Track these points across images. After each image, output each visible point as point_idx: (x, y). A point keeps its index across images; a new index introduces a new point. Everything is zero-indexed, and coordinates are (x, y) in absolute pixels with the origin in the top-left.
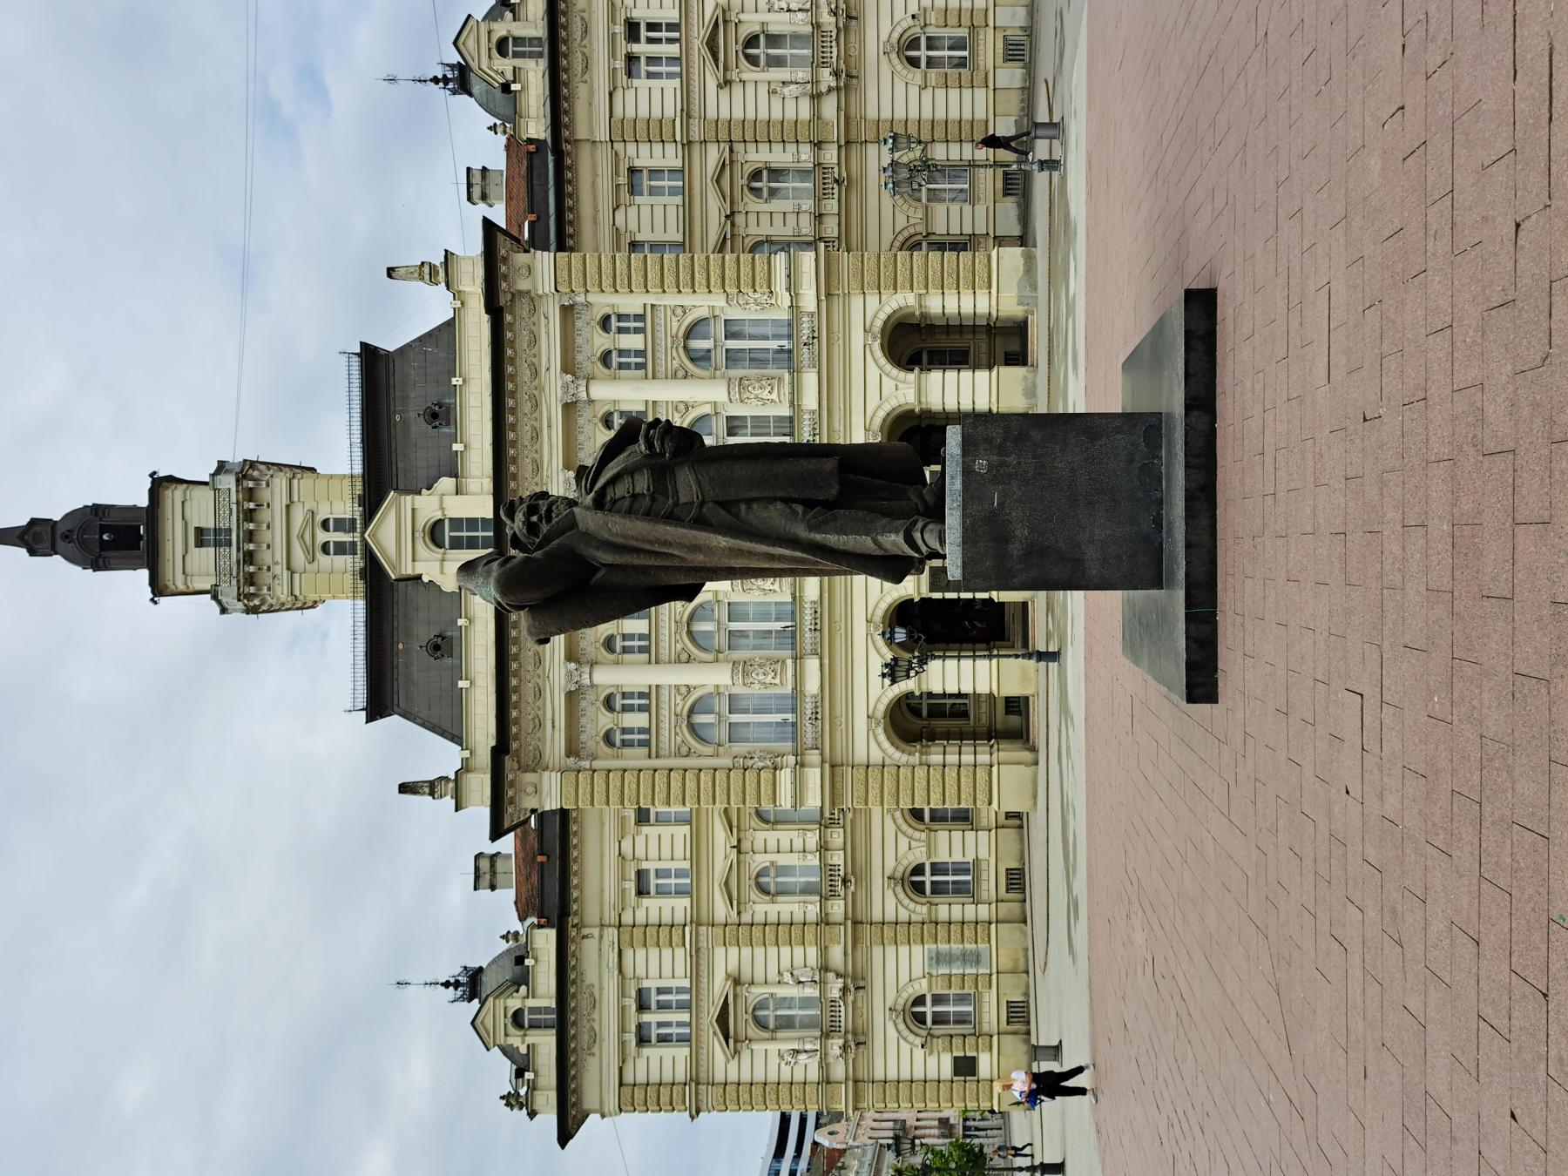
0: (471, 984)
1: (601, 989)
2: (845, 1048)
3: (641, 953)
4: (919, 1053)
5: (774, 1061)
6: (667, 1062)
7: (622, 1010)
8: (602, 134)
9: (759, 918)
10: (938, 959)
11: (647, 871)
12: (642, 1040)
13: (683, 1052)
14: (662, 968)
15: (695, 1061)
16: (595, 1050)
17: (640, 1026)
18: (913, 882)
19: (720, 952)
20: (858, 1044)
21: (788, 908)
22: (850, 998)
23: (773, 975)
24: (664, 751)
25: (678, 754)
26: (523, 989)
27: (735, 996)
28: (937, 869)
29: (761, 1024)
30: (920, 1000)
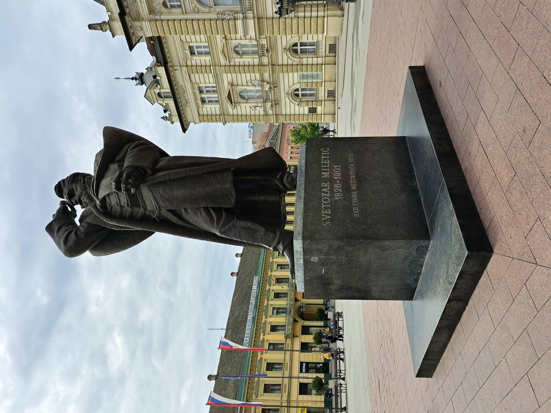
0: (140, 78)
1: (185, 87)
2: (272, 106)
3: (197, 75)
4: (297, 107)
5: (248, 109)
6: (214, 109)
7: (194, 94)
9: (237, 64)
10: (303, 77)
11: (193, 46)
12: (203, 101)
13: (217, 106)
14: (206, 80)
15: (222, 108)
16: (188, 105)
17: (201, 98)
18: (293, 49)
20: (276, 104)
21: (247, 60)
22: (272, 92)
23: (244, 83)
24: (188, 11)
25: (194, 12)
26: (158, 86)
27: (232, 90)
28: (302, 44)
29: (242, 97)
30: (297, 90)
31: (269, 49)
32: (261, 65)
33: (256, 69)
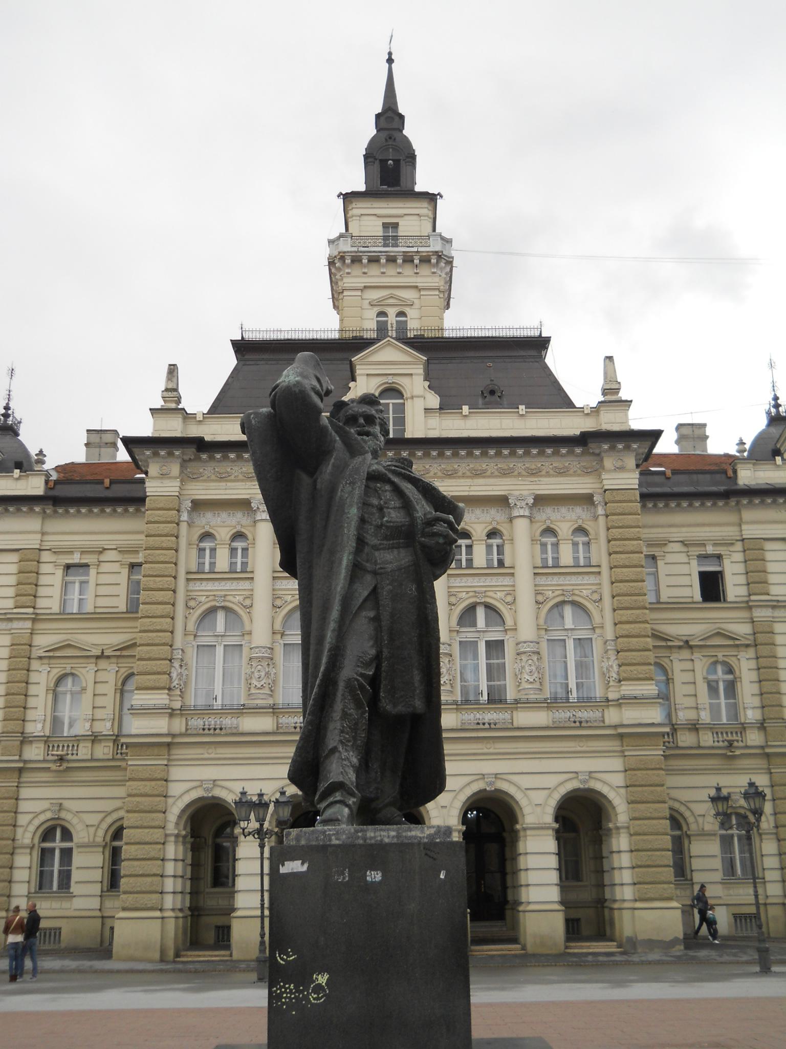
24: (192, 586)
25: (189, 598)
28: (67, 854)
32: (25, 740)
33: (13, 726)
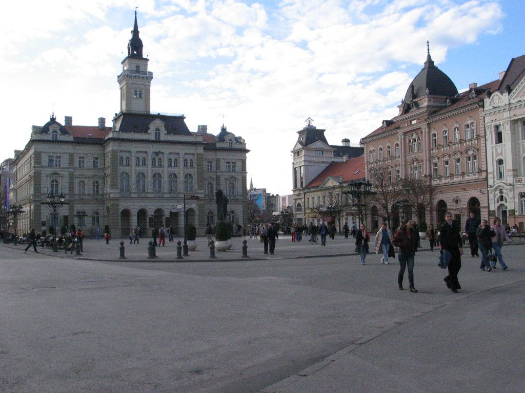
8: (218, 157)
19: (67, 173)
31: (82, 201)
